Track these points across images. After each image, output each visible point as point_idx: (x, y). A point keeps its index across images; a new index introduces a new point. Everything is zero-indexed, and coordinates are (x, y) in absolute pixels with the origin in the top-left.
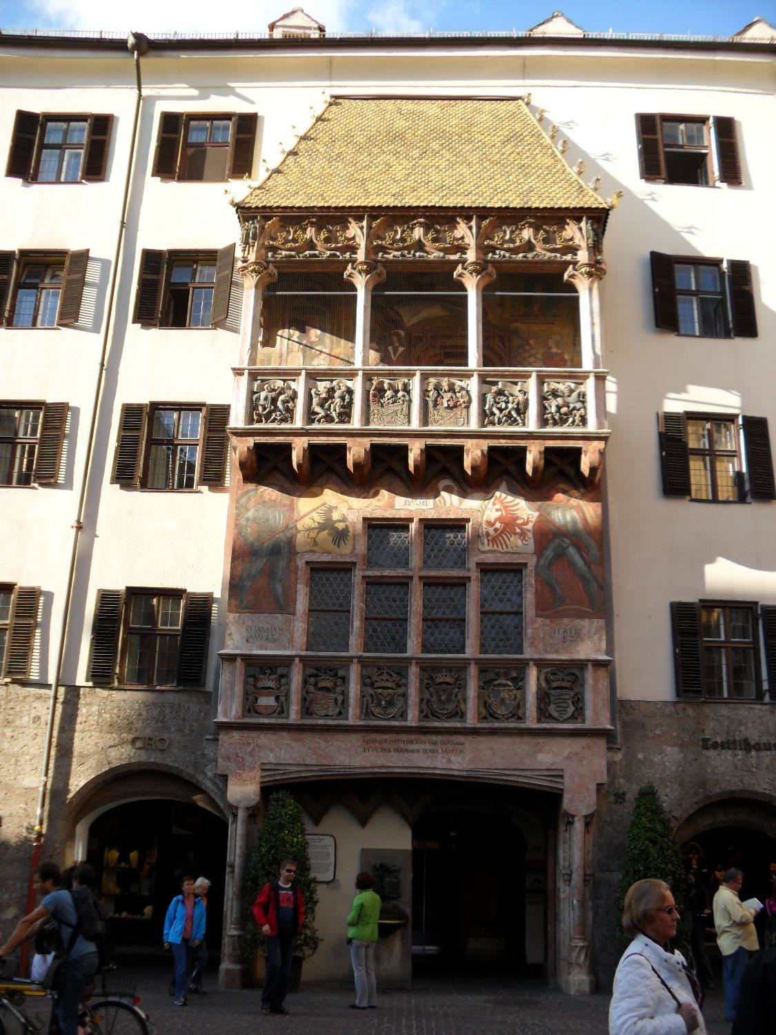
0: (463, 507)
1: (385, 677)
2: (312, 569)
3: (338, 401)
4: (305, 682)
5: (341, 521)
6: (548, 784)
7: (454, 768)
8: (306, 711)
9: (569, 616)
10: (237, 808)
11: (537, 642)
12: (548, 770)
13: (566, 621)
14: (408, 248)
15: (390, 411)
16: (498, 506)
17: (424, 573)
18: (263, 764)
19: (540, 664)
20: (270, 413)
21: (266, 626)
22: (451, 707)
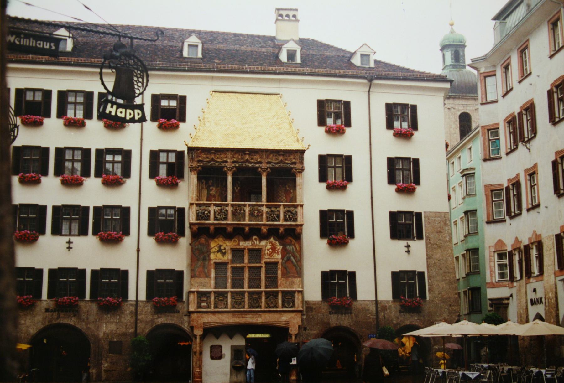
0: (260, 245)
3: (224, 213)
4: (215, 298)
6: (285, 326)
7: (259, 321)
8: (216, 307)
10: (197, 335)
11: (282, 285)
12: (285, 322)
13: (290, 279)
14: (244, 162)
15: (239, 217)
16: (270, 244)
18: (204, 322)
19: (283, 292)
20: (202, 217)
21: (203, 282)
22: (257, 304)
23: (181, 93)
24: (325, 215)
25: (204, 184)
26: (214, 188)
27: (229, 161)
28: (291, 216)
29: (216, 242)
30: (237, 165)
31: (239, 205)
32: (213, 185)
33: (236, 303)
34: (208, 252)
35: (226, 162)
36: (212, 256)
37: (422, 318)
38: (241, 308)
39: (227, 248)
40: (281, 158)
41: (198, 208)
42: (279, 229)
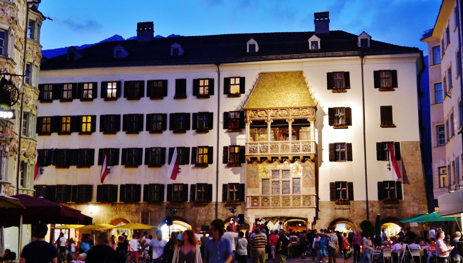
4: (262, 200)
8: (262, 205)
9: (309, 187)
13: (308, 188)
19: (303, 196)
23: (242, 76)
24: (333, 147)
25: (257, 130)
28: (307, 149)
30: (273, 118)
31: (274, 143)
34: (257, 172)
36: (260, 175)
37: (399, 212)
39: (269, 170)
40: (301, 112)
41: (250, 146)
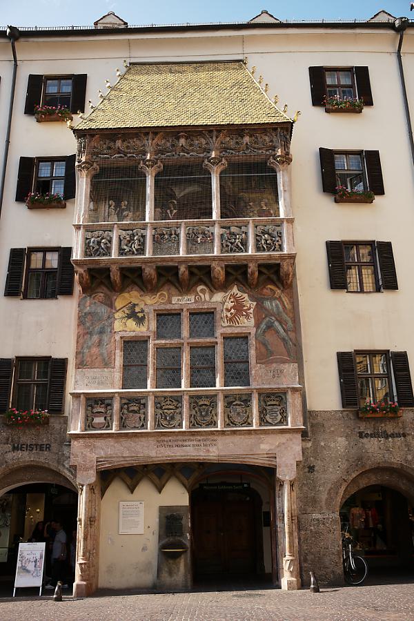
1: (168, 402)
2: (124, 341)
4: (122, 408)
5: (139, 312)
8: (123, 425)
13: (274, 365)
16: (232, 300)
17: (191, 340)
20: (97, 250)
26: (131, 214)
27: (147, 149)
29: (125, 298)
32: (128, 209)
33: (164, 416)
34: (109, 317)
35: (144, 153)
36: (118, 325)
38: (174, 427)
42: (246, 266)
